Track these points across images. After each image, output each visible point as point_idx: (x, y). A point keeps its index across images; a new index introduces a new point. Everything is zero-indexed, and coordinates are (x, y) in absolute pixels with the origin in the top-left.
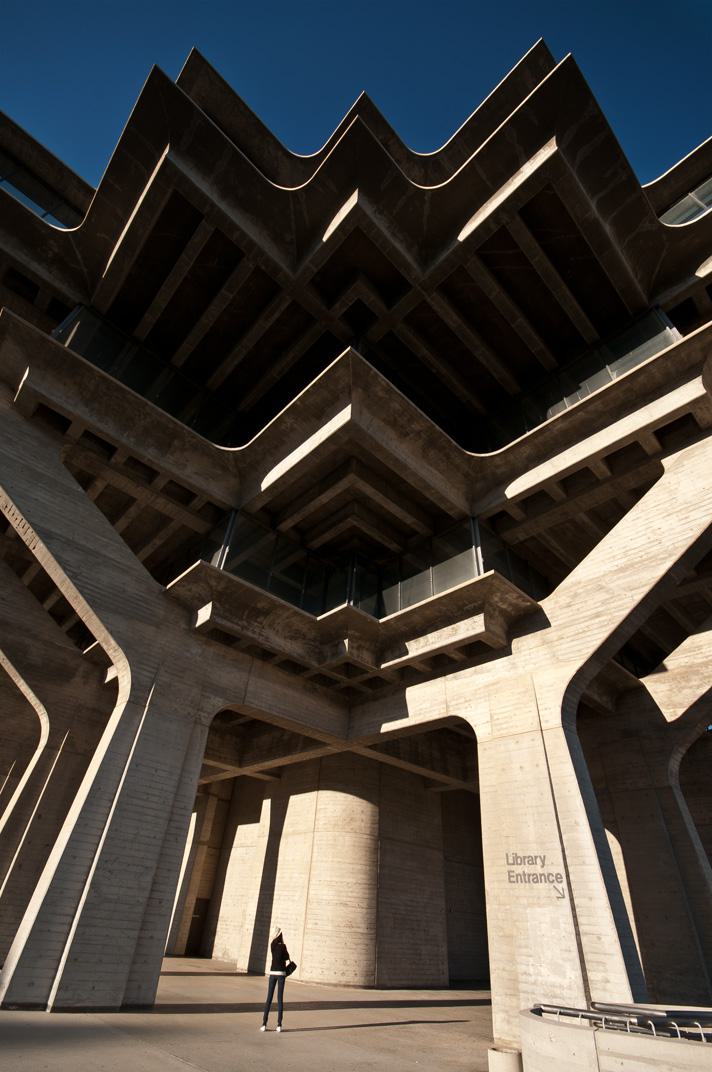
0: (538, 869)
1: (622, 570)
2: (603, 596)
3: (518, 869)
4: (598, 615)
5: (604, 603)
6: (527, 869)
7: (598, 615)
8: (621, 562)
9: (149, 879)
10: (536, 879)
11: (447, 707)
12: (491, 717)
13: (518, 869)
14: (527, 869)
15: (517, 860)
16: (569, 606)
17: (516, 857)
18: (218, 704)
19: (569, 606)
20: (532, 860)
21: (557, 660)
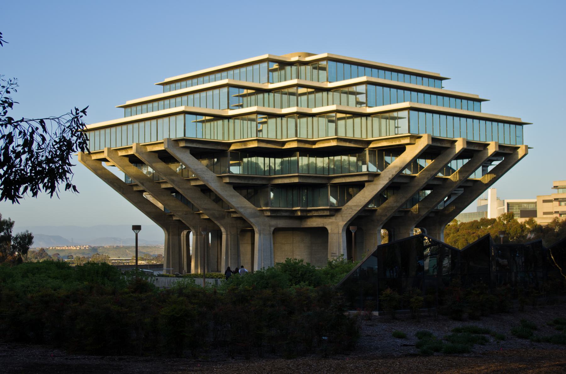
0: (335, 255)
1: (355, 206)
2: (351, 210)
3: (333, 255)
4: (350, 214)
5: (351, 212)
6: (334, 255)
7: (350, 214)
8: (355, 204)
9: (270, 261)
11: (324, 225)
12: (331, 229)
13: (333, 255)
14: (334, 255)
15: (333, 253)
16: (346, 210)
17: (332, 253)
18: (273, 229)
19: (346, 210)
20: (334, 254)
21: (343, 221)
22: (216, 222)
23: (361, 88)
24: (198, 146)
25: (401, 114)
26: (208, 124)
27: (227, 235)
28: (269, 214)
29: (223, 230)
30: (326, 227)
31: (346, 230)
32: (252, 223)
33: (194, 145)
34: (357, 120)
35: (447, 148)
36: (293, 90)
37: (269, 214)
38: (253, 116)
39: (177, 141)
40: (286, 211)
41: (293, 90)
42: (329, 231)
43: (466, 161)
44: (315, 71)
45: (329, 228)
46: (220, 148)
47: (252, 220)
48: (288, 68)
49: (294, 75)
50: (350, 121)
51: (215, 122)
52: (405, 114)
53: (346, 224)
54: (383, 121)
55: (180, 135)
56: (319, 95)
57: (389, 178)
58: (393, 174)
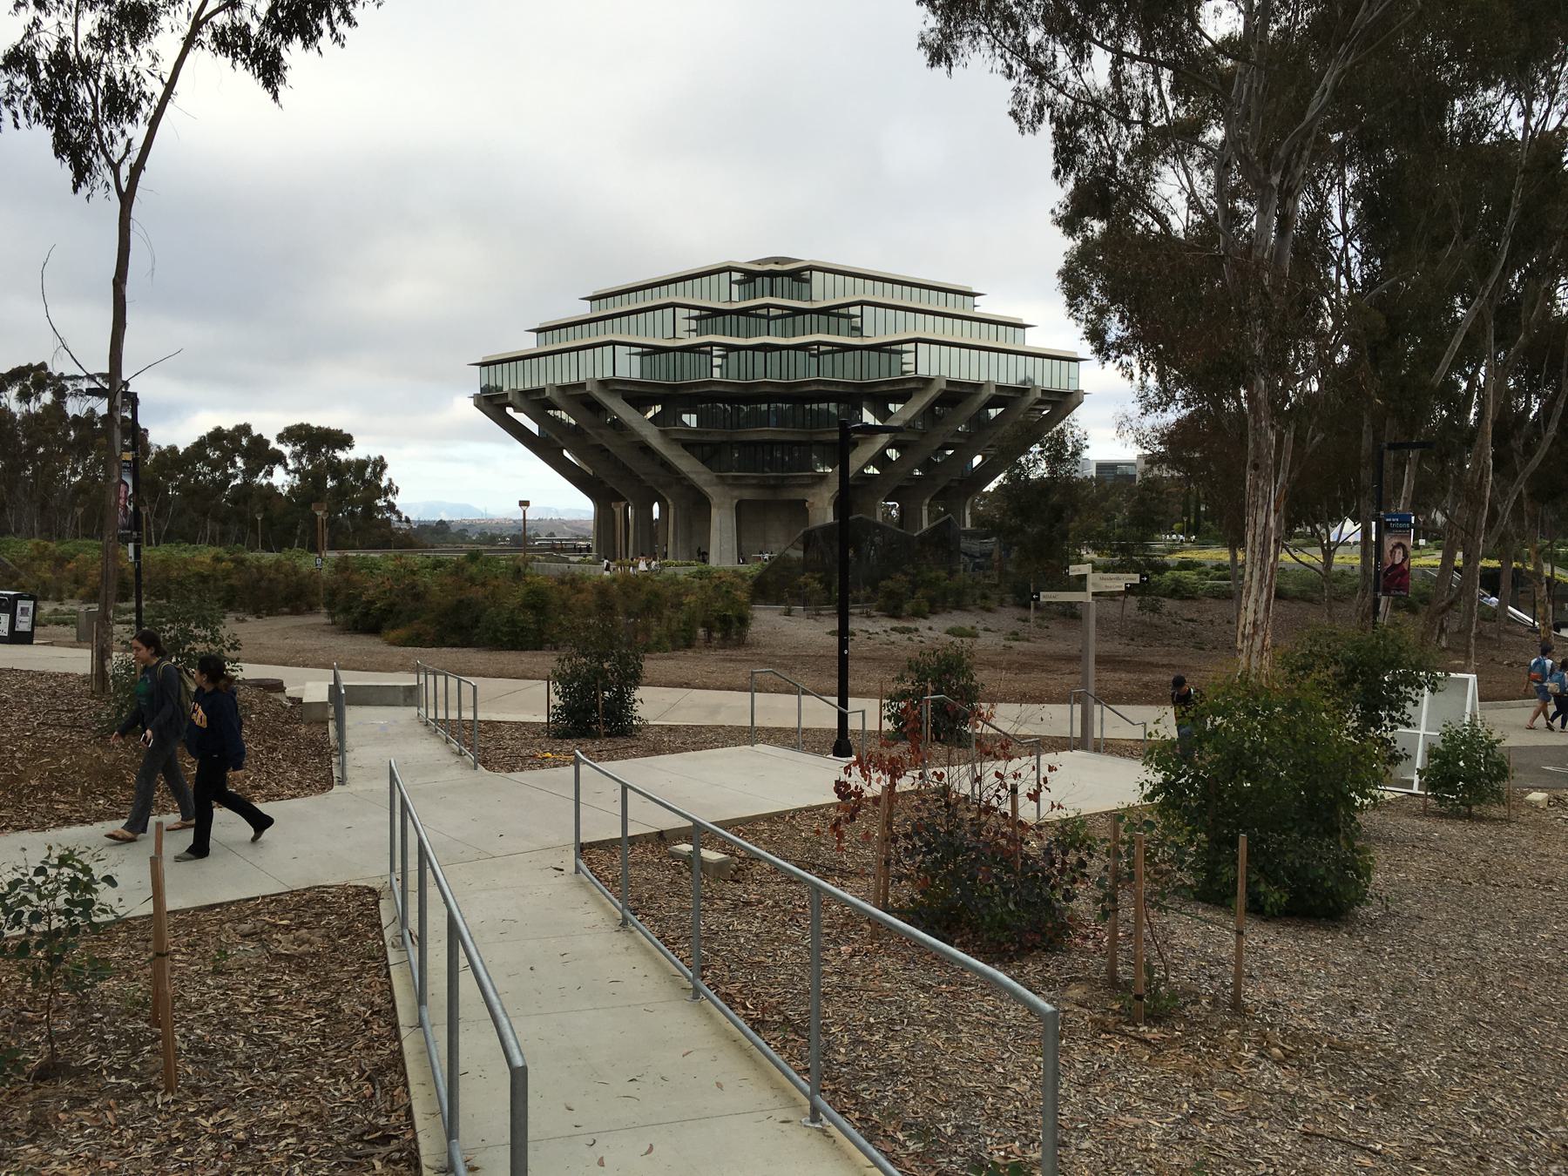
18: (736, 501)
23: (855, 310)
25: (906, 347)
26: (647, 359)
27: (675, 509)
28: (730, 481)
29: (669, 501)
31: (835, 503)
33: (628, 388)
34: (849, 355)
35: (971, 394)
36: (764, 312)
37: (730, 481)
38: (708, 349)
39: (604, 384)
40: (754, 477)
41: (764, 312)
43: (1000, 410)
44: (795, 283)
46: (661, 391)
47: (708, 490)
48: (759, 280)
49: (767, 290)
50: (838, 356)
51: (657, 356)
52: (911, 346)
54: (885, 356)
55: (608, 374)
56: (799, 319)
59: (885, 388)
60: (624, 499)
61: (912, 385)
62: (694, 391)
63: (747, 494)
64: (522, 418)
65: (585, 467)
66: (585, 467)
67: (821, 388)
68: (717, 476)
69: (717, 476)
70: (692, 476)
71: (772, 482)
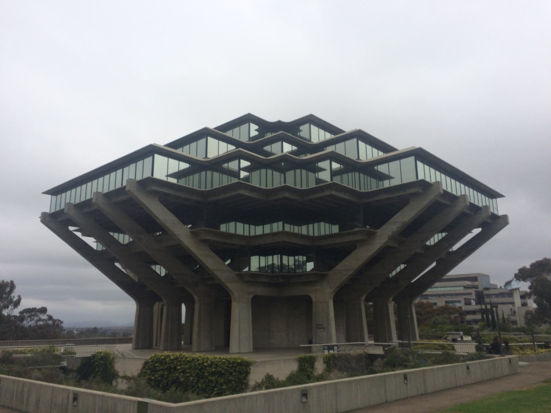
0: (321, 327)
3: (318, 327)
6: (320, 327)
10: (321, 328)
14: (320, 327)
15: (318, 325)
18: (251, 296)
20: (321, 325)
22: (188, 289)
24: (168, 192)
29: (196, 298)
30: (310, 295)
32: (228, 288)
33: (164, 190)
42: (314, 300)
45: (313, 296)
47: (230, 285)
53: (334, 291)
57: (389, 236)
58: (394, 231)
59: (384, 196)
60: (160, 300)
61: (412, 191)
62: (223, 196)
63: (260, 291)
64: (91, 241)
65: (131, 275)
66: (131, 275)
67: (334, 193)
68: (237, 275)
69: (237, 275)
70: (217, 273)
71: (281, 280)
